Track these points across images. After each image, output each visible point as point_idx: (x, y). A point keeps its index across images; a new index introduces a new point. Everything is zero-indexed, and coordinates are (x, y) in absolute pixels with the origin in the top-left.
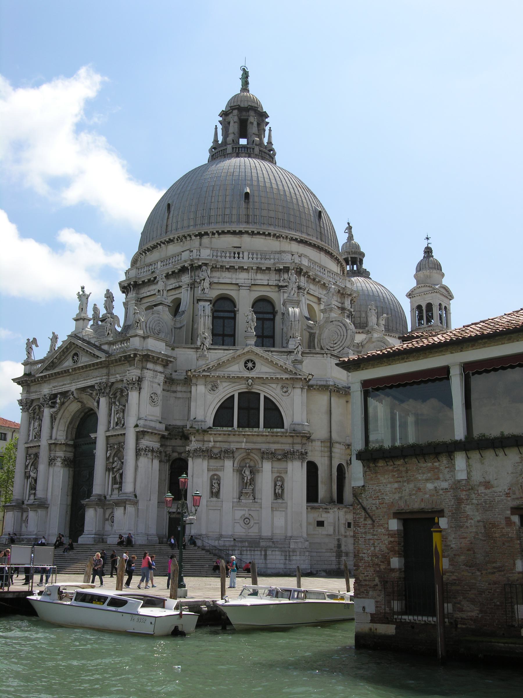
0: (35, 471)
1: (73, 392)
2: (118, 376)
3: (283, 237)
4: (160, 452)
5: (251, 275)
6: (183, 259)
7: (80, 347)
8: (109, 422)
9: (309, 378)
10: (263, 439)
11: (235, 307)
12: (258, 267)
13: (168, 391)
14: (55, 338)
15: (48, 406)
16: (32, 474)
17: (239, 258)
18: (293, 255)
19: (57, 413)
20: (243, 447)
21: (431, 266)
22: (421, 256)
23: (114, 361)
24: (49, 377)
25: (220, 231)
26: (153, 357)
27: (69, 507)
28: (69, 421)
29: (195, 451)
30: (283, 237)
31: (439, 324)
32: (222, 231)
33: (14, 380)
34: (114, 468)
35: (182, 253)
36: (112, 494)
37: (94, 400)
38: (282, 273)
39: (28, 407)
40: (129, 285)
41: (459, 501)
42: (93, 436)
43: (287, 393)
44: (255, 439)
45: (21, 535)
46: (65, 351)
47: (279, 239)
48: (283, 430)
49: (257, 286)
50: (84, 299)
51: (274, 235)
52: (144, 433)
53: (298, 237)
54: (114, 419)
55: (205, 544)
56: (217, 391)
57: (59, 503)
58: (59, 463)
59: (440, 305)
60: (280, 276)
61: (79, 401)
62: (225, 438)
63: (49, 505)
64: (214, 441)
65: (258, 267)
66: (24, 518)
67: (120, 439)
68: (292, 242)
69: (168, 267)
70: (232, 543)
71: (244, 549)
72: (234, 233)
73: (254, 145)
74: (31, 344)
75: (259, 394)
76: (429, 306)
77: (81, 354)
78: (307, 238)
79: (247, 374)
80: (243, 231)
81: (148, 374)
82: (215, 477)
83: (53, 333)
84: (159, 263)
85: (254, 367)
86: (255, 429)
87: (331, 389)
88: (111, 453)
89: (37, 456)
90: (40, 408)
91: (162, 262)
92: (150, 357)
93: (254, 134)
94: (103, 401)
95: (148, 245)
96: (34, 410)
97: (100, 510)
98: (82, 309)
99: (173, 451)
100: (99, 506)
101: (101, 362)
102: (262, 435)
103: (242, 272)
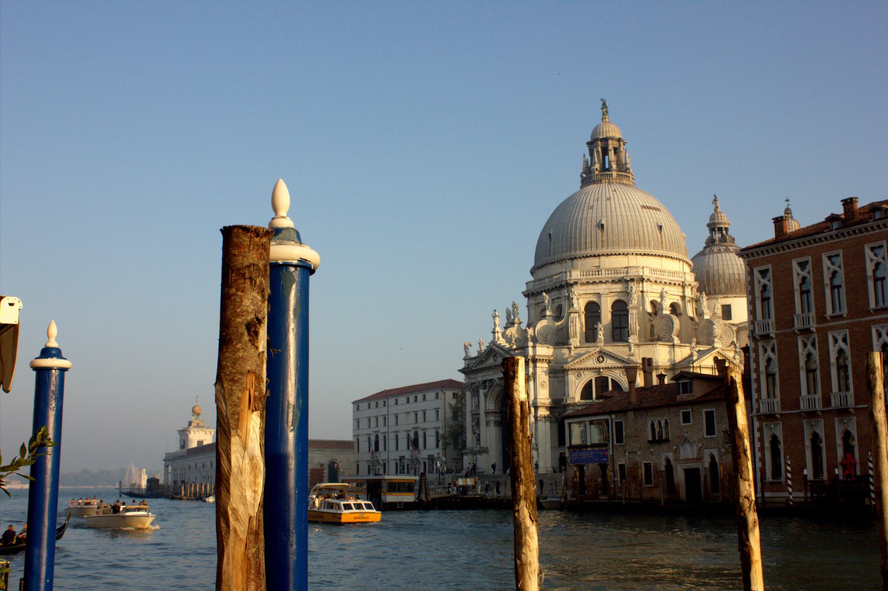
4: (550, 417)
5: (609, 285)
13: (553, 377)
16: (477, 432)
17: (599, 274)
27: (502, 452)
33: (459, 371)
38: (629, 283)
40: (528, 294)
58: (492, 424)
68: (638, 256)
72: (595, 256)
75: (607, 378)
84: (547, 279)
89: (478, 420)
90: (477, 389)
95: (541, 263)
96: (474, 389)
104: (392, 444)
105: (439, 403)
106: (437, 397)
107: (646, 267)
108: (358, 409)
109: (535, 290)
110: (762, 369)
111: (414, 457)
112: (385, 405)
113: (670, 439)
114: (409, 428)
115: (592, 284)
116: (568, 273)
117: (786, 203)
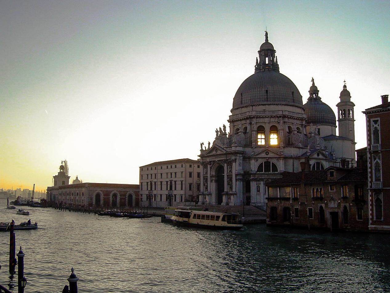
14: (209, 143)
16: (206, 184)
19: (212, 167)
29: (252, 179)
33: (198, 156)
41: (278, 206)
44: (269, 175)
48: (277, 172)
52: (238, 175)
67: (231, 176)
72: (263, 105)
79: (266, 156)
86: (269, 172)
89: (207, 179)
90: (206, 165)
96: (205, 165)
97: (227, 196)
99: (246, 178)
104: (159, 187)
105: (183, 169)
106: (182, 167)
107: (287, 111)
108: (142, 170)
110: (373, 168)
111: (170, 193)
112: (156, 169)
113: (323, 196)
114: (168, 180)
117: (344, 83)
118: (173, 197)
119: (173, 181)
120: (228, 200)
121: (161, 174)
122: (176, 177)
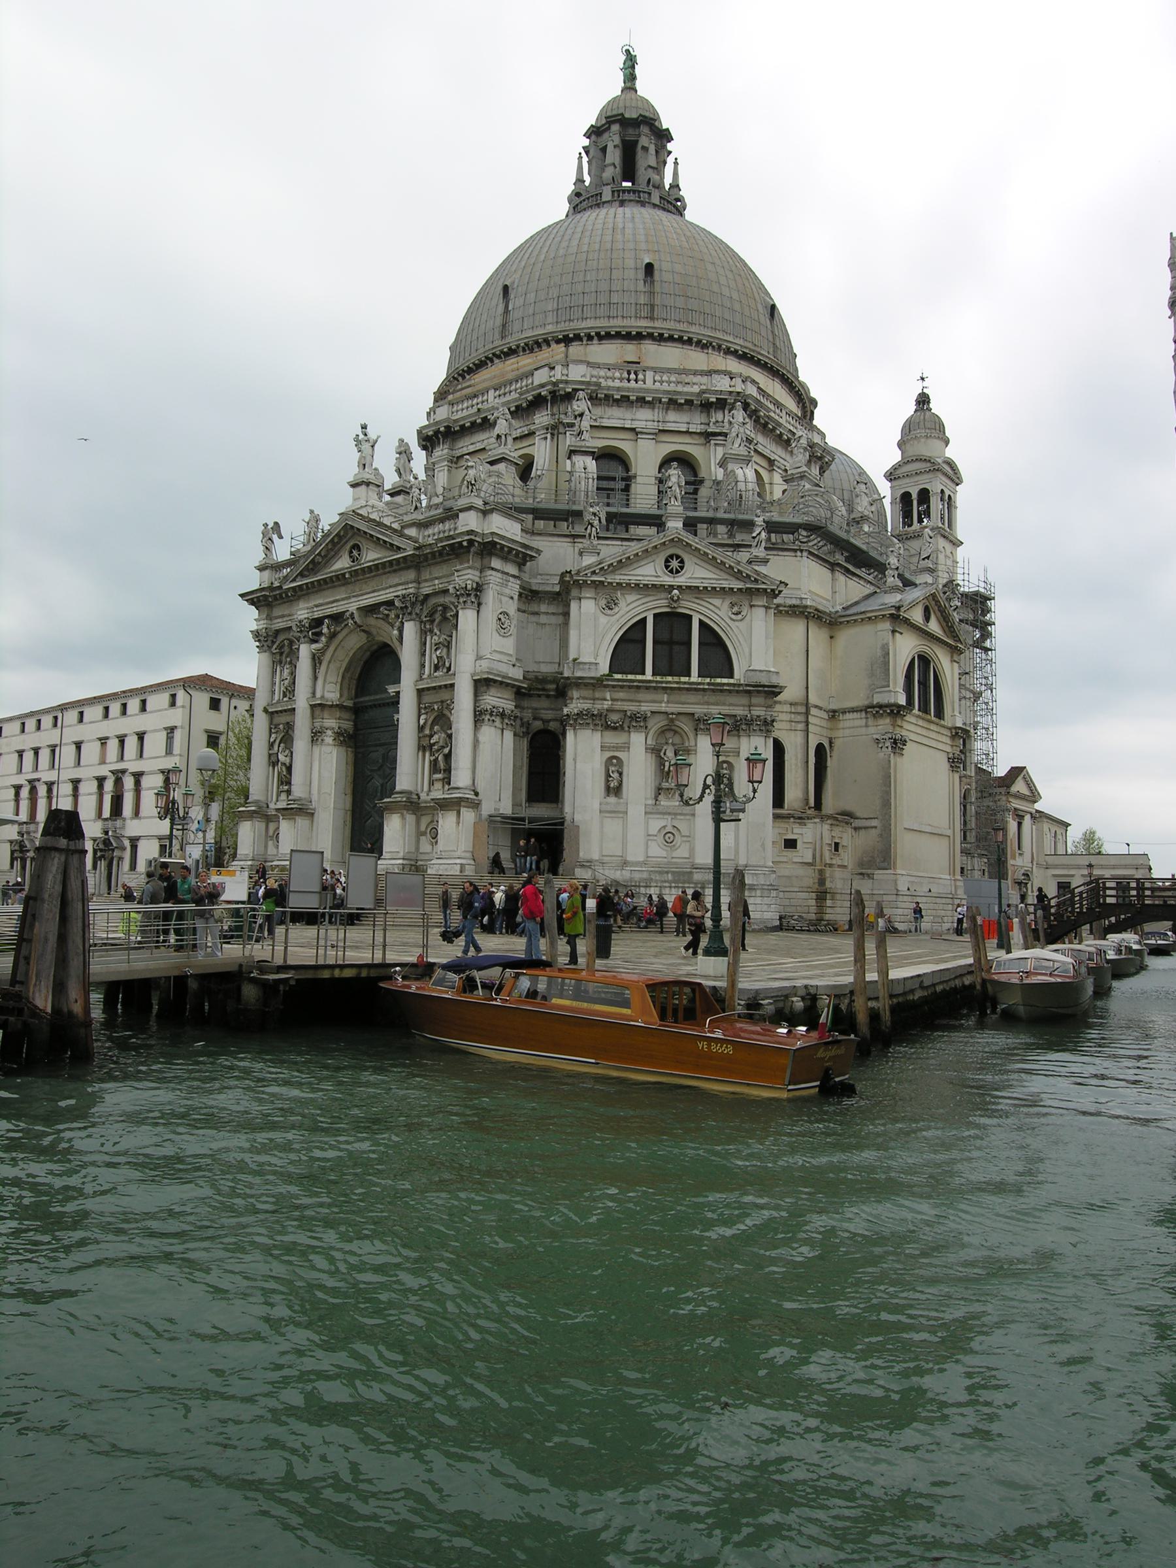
0: (287, 751)
1: (353, 613)
2: (437, 582)
3: (713, 347)
4: (516, 717)
6: (536, 383)
7: (365, 533)
8: (423, 666)
9: (780, 589)
10: (697, 698)
11: (627, 469)
12: (670, 400)
15: (306, 639)
16: (281, 757)
17: (636, 381)
18: (731, 378)
19: (323, 651)
20: (663, 709)
21: (928, 425)
22: (911, 408)
23: (429, 556)
24: (307, 587)
25: (603, 333)
26: (503, 546)
27: (349, 813)
28: (344, 665)
29: (580, 715)
30: (713, 347)
31: (940, 525)
32: (606, 333)
33: (242, 596)
34: (434, 744)
35: (535, 373)
36: (430, 790)
37: (392, 626)
39: (269, 643)
40: (437, 432)
42: (392, 690)
43: (740, 617)
44: (684, 697)
45: (265, 861)
46: (336, 540)
47: (706, 351)
48: (731, 681)
49: (667, 434)
50: (366, 447)
51: (699, 342)
53: (739, 348)
54: (431, 658)
55: (599, 876)
56: (616, 609)
57: (332, 805)
58: (329, 738)
59: (942, 491)
60: (708, 413)
61: (363, 631)
62: (630, 695)
63: (314, 809)
64: (612, 700)
65: (670, 400)
66: (271, 833)
69: (508, 398)
70: (645, 875)
71: (667, 884)
72: (628, 337)
73: (651, 187)
74: (273, 531)
75: (691, 617)
76: (924, 495)
77: (365, 547)
78: (753, 351)
79: (668, 580)
80: (644, 333)
81: (493, 578)
82: (615, 761)
83: (312, 512)
84: (491, 392)
85: (682, 568)
86: (683, 679)
87: (809, 613)
88: (426, 720)
89: (289, 727)
90: (291, 643)
91: (496, 390)
92: (498, 546)
93: (650, 167)
94: (410, 630)
96: (281, 647)
97: (410, 818)
98: (364, 465)
99: (535, 719)
100: (408, 810)
101: (404, 558)
102: (696, 690)
103: (641, 406)
105: (176, 717)
106: (173, 704)
109: (456, 421)
111: (110, 833)
112: (55, 725)
114: (104, 771)
115: (617, 402)
116: (558, 368)
117: (920, 384)
118: (124, 849)
119: (127, 774)
120: (418, 841)
121: (78, 746)
122: (141, 756)
